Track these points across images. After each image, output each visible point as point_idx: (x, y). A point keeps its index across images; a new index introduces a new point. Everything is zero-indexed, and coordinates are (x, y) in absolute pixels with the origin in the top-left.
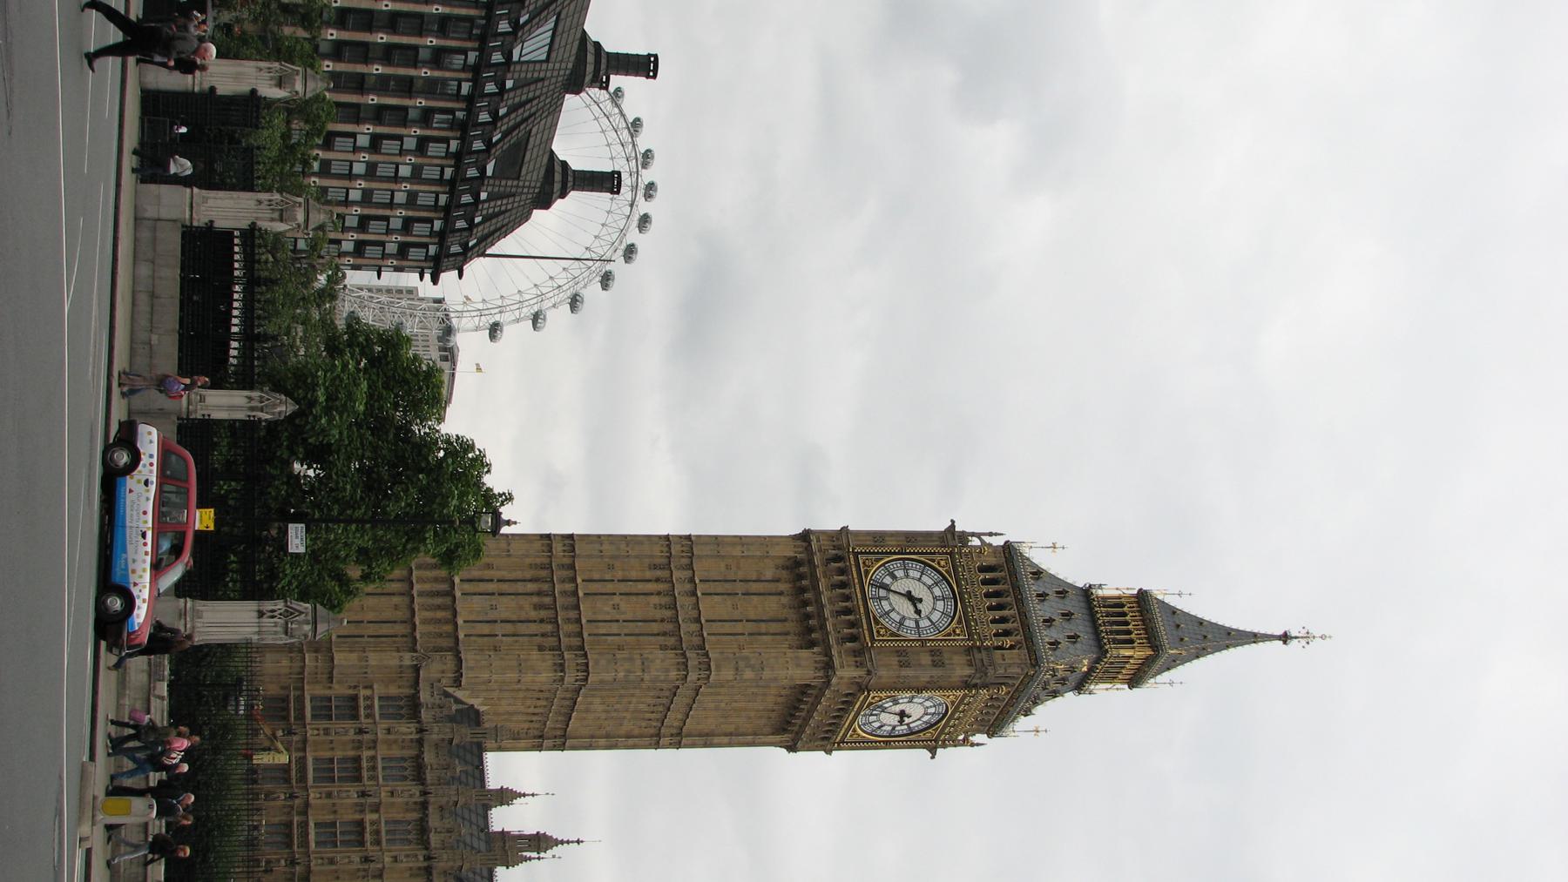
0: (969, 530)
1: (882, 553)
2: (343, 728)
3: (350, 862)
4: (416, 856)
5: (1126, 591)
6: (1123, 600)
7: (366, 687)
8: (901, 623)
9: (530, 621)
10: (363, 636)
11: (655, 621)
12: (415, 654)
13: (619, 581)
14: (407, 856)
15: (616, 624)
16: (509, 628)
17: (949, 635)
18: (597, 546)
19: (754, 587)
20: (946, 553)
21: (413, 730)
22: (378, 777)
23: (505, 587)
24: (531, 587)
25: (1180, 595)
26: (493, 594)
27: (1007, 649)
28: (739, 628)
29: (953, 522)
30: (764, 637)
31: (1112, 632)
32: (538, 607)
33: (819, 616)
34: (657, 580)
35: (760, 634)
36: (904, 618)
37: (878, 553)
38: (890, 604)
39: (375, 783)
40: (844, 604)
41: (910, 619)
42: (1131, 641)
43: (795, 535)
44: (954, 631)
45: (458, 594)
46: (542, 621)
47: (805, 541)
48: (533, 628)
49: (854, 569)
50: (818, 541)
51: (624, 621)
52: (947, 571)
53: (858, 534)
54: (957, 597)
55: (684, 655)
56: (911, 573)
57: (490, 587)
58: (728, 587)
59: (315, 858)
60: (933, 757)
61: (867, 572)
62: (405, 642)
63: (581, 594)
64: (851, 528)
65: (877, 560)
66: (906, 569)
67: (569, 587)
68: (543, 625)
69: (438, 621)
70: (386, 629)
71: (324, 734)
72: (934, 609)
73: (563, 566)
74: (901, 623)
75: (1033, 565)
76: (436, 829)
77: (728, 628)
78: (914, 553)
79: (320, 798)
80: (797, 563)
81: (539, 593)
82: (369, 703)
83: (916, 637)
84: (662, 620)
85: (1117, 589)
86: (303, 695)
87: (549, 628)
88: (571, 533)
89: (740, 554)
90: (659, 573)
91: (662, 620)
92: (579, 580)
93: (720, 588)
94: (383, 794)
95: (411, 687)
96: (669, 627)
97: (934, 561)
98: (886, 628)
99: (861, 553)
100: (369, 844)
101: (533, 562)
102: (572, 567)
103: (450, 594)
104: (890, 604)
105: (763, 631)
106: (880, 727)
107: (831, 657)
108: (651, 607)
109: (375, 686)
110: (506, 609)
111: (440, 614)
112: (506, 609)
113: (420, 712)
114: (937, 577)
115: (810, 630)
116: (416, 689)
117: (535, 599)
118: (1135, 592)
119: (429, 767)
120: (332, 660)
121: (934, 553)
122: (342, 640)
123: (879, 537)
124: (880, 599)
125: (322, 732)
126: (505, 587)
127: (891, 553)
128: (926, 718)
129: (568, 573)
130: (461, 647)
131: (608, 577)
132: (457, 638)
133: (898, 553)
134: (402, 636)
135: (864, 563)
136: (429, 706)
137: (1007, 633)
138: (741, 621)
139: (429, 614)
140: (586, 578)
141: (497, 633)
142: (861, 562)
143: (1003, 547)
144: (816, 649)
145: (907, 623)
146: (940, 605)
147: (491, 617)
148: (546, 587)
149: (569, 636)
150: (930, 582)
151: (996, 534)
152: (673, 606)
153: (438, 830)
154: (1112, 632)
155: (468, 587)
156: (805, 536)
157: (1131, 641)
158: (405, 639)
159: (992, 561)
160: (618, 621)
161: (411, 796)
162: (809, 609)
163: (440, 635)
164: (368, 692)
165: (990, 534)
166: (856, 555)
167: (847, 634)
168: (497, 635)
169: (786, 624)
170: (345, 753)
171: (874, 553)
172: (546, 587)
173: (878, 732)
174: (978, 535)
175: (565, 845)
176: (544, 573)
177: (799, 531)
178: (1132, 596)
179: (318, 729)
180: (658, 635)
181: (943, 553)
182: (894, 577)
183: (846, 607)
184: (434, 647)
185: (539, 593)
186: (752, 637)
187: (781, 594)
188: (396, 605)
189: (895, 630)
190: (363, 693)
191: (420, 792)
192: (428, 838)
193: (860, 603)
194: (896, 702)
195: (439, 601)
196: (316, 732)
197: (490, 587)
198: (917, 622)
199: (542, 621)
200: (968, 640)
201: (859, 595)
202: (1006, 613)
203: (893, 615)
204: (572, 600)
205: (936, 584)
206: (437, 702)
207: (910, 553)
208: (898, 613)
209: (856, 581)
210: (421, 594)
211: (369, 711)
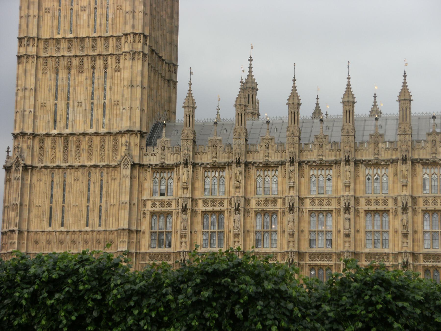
2: (181, 222)
3: (293, 222)
4: (290, 172)
7: (145, 205)
9: (93, 77)
10: (100, 206)
12: (122, 166)
13: (60, 6)
14: (290, 178)
16: (98, 94)
18: (31, 19)
21: (185, 170)
22: (221, 199)
23: (62, 95)
26: (68, 104)
32: (81, 70)
39: (226, 201)
45: (68, 131)
46: (93, 68)
48: (99, 73)
51: (96, 4)
57: (61, 105)
59: (289, 247)
62: (108, 173)
67: (64, 45)
68: (97, 67)
69: (90, 147)
70: (95, 188)
71: (185, 238)
76: (266, 156)
79: (239, 242)
81: (69, 68)
82: (158, 204)
86: (150, 254)
87: (99, 63)
92: (59, 36)
94: (237, 194)
95: (146, 171)
100: (276, 207)
101: (41, 71)
102: (46, 41)
103: (66, 138)
109: (145, 197)
111: (84, 145)
113: (168, 165)
116: (149, 167)
117: (73, 71)
119: (214, 159)
120: (124, 230)
122: (103, 223)
125: (183, 240)
126: (62, 95)
129: (52, 45)
130: (115, 130)
131: (56, 14)
132: (109, 134)
134: (102, 176)
136: (163, 157)
139: (84, 155)
140: (55, 31)
141: (103, 102)
147: (89, 107)
153: (267, 154)
155: (61, 124)
158: (105, 174)
160: (96, 8)
161: (240, 173)
163: (102, 146)
164: (149, 204)
168: (105, 103)
170: (200, 223)
172: (63, 63)
176: (51, 64)
179: (181, 243)
184: (113, 152)
188: (75, 180)
190: (149, 207)
191: (237, 167)
192: (273, 162)
195: (72, 147)
196: (183, 244)
197: (61, 105)
199: (93, 68)
204: (76, 44)
206: (160, 151)
210: (65, 160)
211: (165, 204)
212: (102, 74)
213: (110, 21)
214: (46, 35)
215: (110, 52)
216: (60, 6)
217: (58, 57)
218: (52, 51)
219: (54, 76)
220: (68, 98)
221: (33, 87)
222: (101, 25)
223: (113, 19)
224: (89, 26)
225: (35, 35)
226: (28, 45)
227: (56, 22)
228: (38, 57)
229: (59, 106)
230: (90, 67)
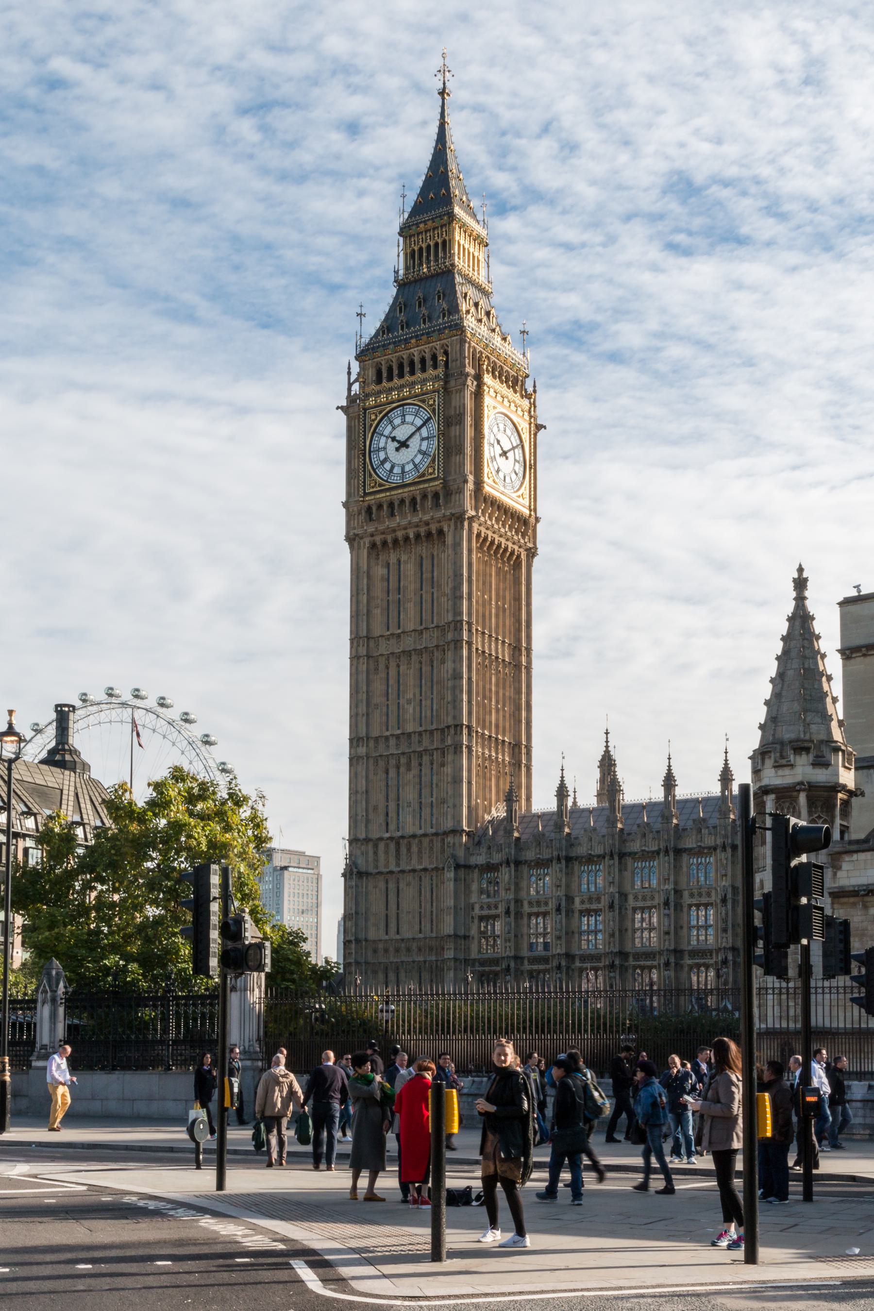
0: (346, 394)
1: (364, 471)
5: (401, 248)
6: (408, 251)
8: (424, 453)
11: (421, 669)
13: (388, 700)
15: (423, 702)
16: (425, 792)
17: (434, 410)
18: (359, 718)
19: (393, 584)
20: (365, 413)
23: (392, 795)
24: (392, 773)
25: (404, 197)
27: (447, 359)
28: (427, 597)
29: (338, 408)
30: (435, 574)
31: (436, 260)
33: (417, 526)
34: (387, 667)
35: (433, 577)
36: (420, 451)
37: (364, 475)
38: (408, 463)
40: (407, 504)
41: (420, 445)
42: (444, 242)
43: (350, 548)
44: (431, 405)
46: (420, 765)
47: (354, 540)
48: (426, 770)
49: (378, 496)
50: (354, 528)
52: (380, 413)
53: (349, 494)
54: (402, 403)
55: (448, 643)
56: (382, 445)
58: (393, 607)
60: (545, 427)
61: (381, 485)
63: (399, 732)
64: (344, 500)
65: (371, 475)
66: (379, 450)
67: (392, 742)
72: (412, 424)
73: (376, 747)
74: (424, 453)
75: (376, 335)
77: (426, 606)
78: (365, 443)
80: (373, 546)
81: (398, 767)
83: (436, 439)
84: (421, 663)
85: (398, 256)
87: (426, 759)
88: (348, 741)
89: (365, 596)
90: (382, 666)
91: (421, 663)
92: (388, 733)
93: (393, 614)
96: (425, 657)
97: (371, 425)
98: (428, 467)
99: (364, 490)
102: (376, 739)
104: (408, 463)
105: (429, 575)
106: (516, 474)
107: (453, 515)
108: (409, 673)
110: (409, 794)
112: (409, 794)
114: (385, 422)
115: (429, 534)
117: (402, 770)
118: (401, 239)
121: (365, 424)
123: (351, 474)
124: (403, 472)
126: (392, 795)
127: (364, 464)
128: (508, 432)
131: (384, 709)
133: (364, 455)
135: (373, 487)
137: (434, 358)
138: (421, 595)
140: (384, 728)
142: (371, 490)
143: (360, 362)
144: (445, 529)
145: (424, 448)
146: (409, 418)
148: (393, 762)
149: (433, 741)
150: (389, 428)
151: (349, 368)
152: (408, 654)
154: (436, 260)
156: (352, 539)
157: (444, 242)
159: (371, 374)
160: (421, 700)
162: (411, 536)
165: (349, 373)
166: (366, 494)
167: (432, 501)
169: (424, 556)
171: (364, 479)
172: (393, 762)
173: (521, 475)
174: (350, 385)
175: (609, 744)
176: (381, 763)
177: (346, 545)
178: (405, 242)
180: (432, 666)
181: (365, 417)
182: (386, 460)
183: (410, 503)
185: (398, 767)
186: (435, 584)
187: (399, 561)
189: (430, 459)
193: (406, 490)
194: (493, 459)
198: (423, 439)
200: (438, 392)
201: (400, 491)
202: (417, 359)
203: (417, 461)
205: (391, 422)
207: (365, 446)
208: (416, 456)
209: (388, 494)
212: (428, 772)
213: (434, 713)
214: (375, 733)
215: (435, 747)
216: (388, 700)
217: (387, 756)
218: (382, 750)
219: (384, 776)
220: (398, 800)
221: (364, 789)
222: (426, 717)
223: (437, 710)
224: (414, 719)
225: (364, 734)
226: (358, 746)
227: (384, 718)
228: (368, 758)
229: (390, 808)
230: (417, 765)
